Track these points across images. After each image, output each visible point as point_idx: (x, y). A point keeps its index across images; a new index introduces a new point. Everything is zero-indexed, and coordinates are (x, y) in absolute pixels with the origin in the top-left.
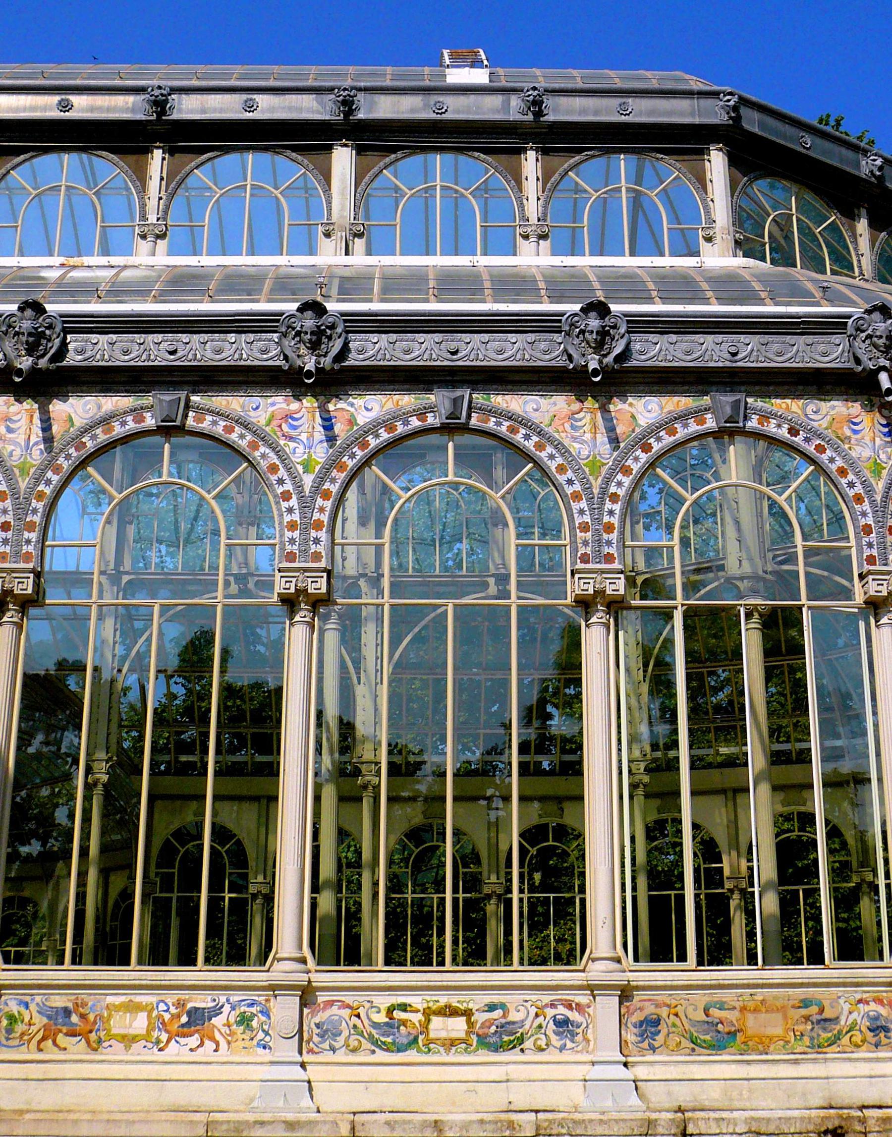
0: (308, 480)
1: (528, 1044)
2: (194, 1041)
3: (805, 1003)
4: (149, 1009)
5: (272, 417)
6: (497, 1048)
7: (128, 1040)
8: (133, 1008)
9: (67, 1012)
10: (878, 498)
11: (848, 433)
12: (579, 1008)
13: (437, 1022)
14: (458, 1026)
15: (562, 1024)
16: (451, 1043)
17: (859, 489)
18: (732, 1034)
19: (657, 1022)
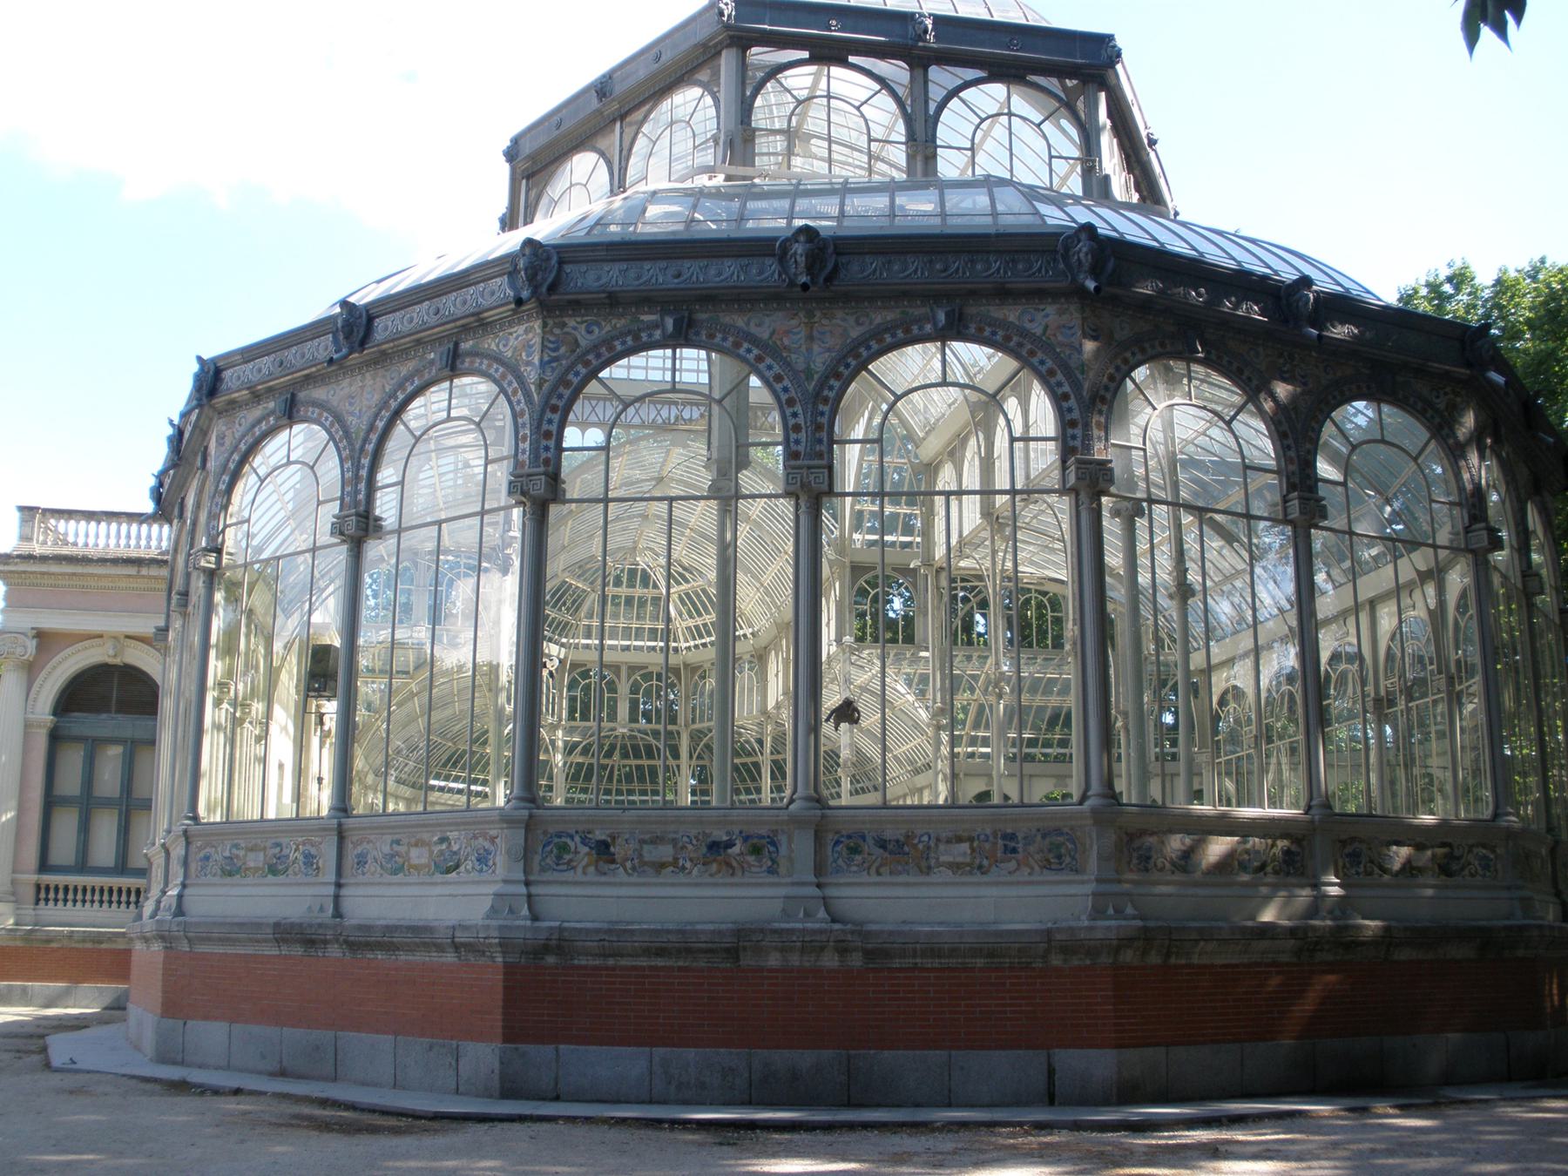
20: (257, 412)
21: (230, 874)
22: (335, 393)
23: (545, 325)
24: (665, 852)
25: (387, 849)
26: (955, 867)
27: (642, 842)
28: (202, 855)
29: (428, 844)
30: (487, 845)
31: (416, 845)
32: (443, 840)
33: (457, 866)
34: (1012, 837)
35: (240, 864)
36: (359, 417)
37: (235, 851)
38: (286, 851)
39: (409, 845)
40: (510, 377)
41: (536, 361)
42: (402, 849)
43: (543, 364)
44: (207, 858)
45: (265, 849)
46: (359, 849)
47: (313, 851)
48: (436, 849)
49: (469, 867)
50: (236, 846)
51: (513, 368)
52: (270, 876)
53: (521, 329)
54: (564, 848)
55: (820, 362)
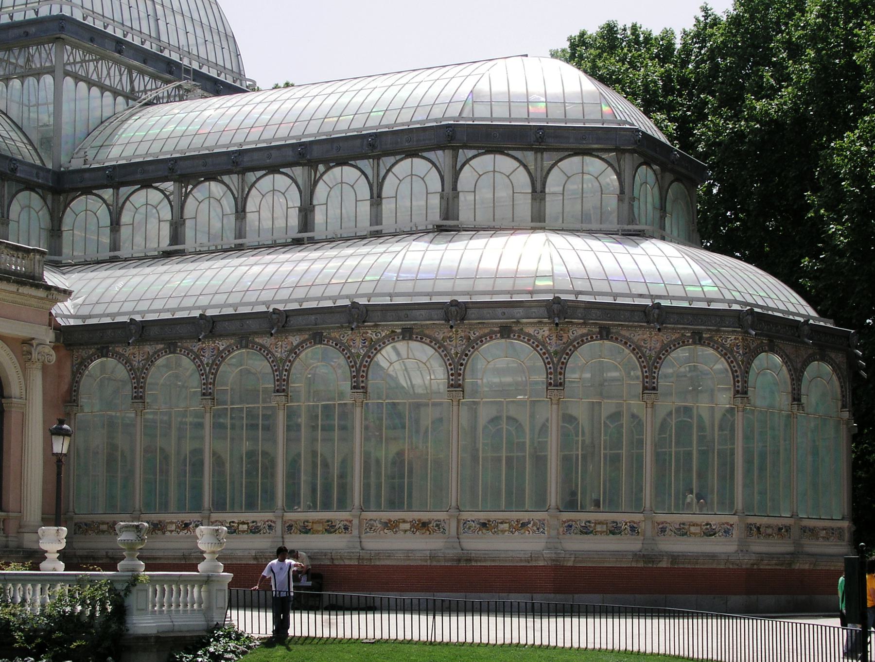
0: (208, 369)
1: (262, 532)
2: (186, 531)
3: (328, 521)
4: (175, 523)
5: (199, 349)
6: (254, 533)
7: (171, 531)
8: (172, 523)
9: (157, 524)
10: (358, 366)
11: (352, 344)
12: (274, 522)
13: (240, 526)
14: (245, 527)
15: (270, 527)
16: (243, 532)
17: (353, 363)
18: (310, 530)
19: (292, 526)
20: (584, 331)
21: (586, 533)
22: (638, 336)
23: (743, 339)
24: (769, 531)
25: (678, 527)
26: (823, 537)
27: (766, 527)
28: (566, 524)
29: (701, 525)
30: (729, 527)
31: (694, 525)
32: (707, 524)
33: (714, 534)
34: (833, 529)
35: (591, 529)
36: (650, 350)
37: (587, 524)
38: (619, 525)
39: (689, 525)
40: (729, 355)
41: (741, 352)
42: (686, 527)
43: (744, 354)
44: (571, 526)
45: (607, 523)
46: (661, 526)
47: (635, 525)
48: (704, 528)
49: (721, 534)
50: (589, 522)
51: (732, 352)
52: (611, 535)
53: (733, 337)
54: (751, 528)
55: (799, 366)
